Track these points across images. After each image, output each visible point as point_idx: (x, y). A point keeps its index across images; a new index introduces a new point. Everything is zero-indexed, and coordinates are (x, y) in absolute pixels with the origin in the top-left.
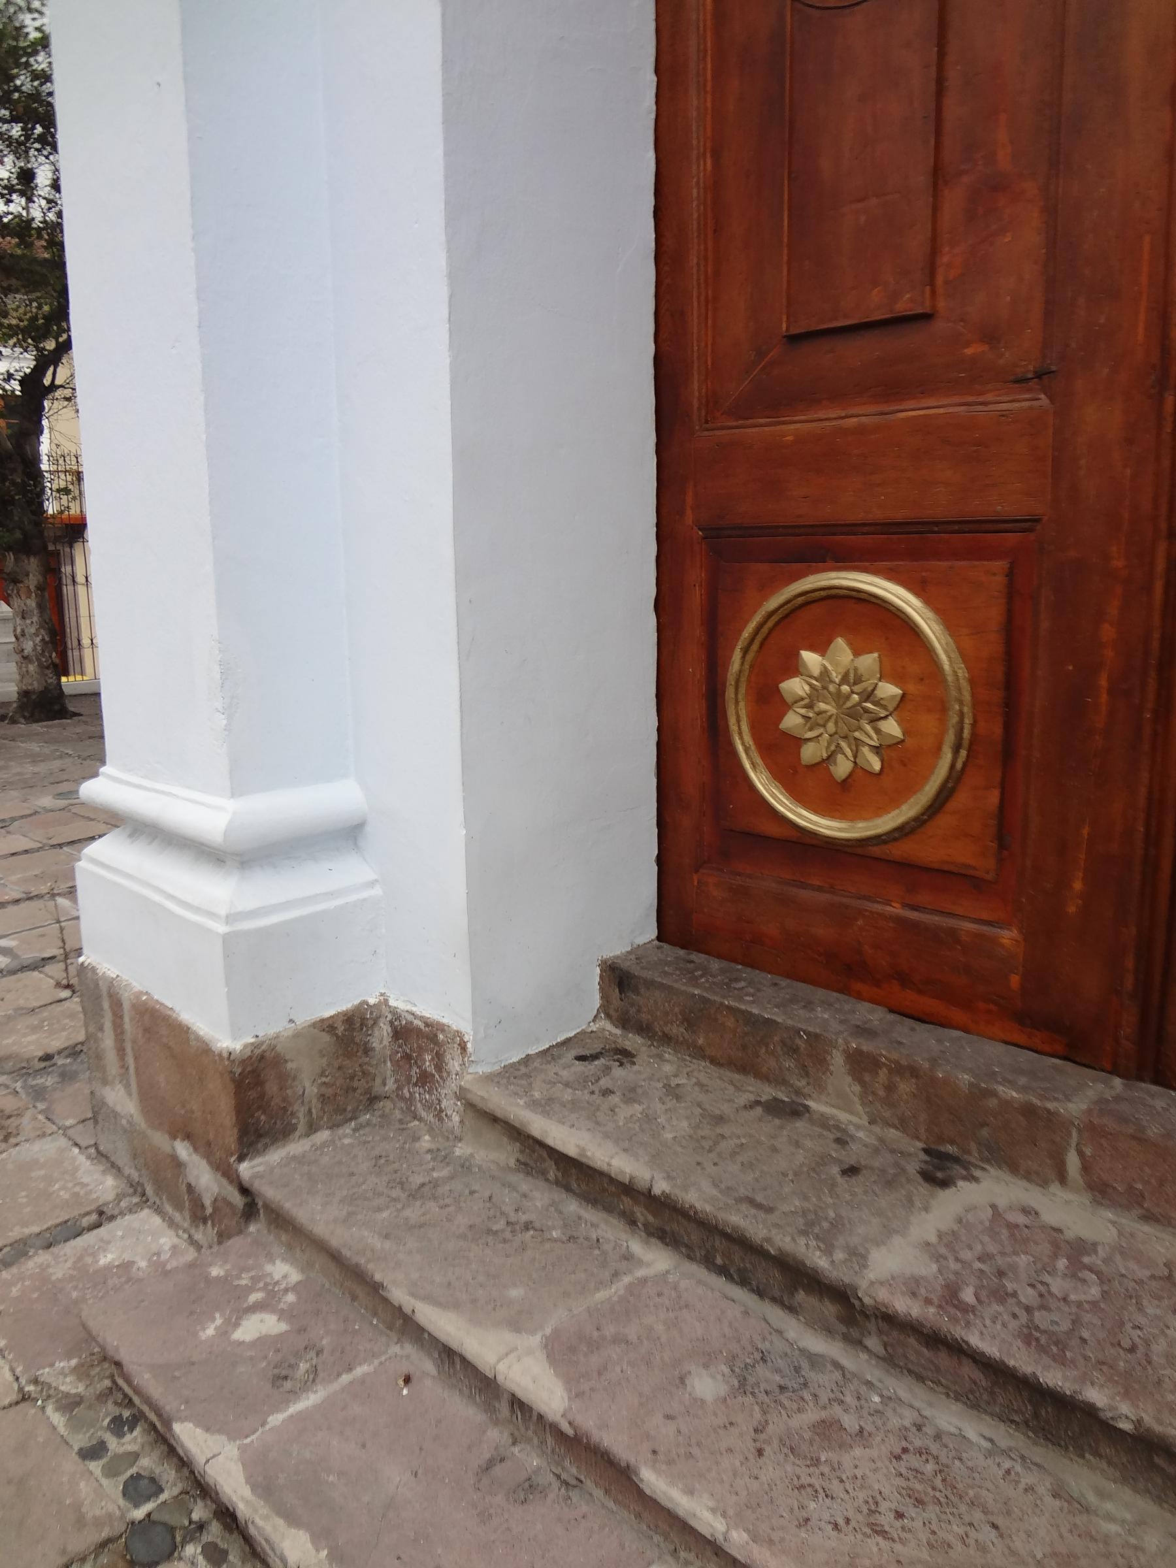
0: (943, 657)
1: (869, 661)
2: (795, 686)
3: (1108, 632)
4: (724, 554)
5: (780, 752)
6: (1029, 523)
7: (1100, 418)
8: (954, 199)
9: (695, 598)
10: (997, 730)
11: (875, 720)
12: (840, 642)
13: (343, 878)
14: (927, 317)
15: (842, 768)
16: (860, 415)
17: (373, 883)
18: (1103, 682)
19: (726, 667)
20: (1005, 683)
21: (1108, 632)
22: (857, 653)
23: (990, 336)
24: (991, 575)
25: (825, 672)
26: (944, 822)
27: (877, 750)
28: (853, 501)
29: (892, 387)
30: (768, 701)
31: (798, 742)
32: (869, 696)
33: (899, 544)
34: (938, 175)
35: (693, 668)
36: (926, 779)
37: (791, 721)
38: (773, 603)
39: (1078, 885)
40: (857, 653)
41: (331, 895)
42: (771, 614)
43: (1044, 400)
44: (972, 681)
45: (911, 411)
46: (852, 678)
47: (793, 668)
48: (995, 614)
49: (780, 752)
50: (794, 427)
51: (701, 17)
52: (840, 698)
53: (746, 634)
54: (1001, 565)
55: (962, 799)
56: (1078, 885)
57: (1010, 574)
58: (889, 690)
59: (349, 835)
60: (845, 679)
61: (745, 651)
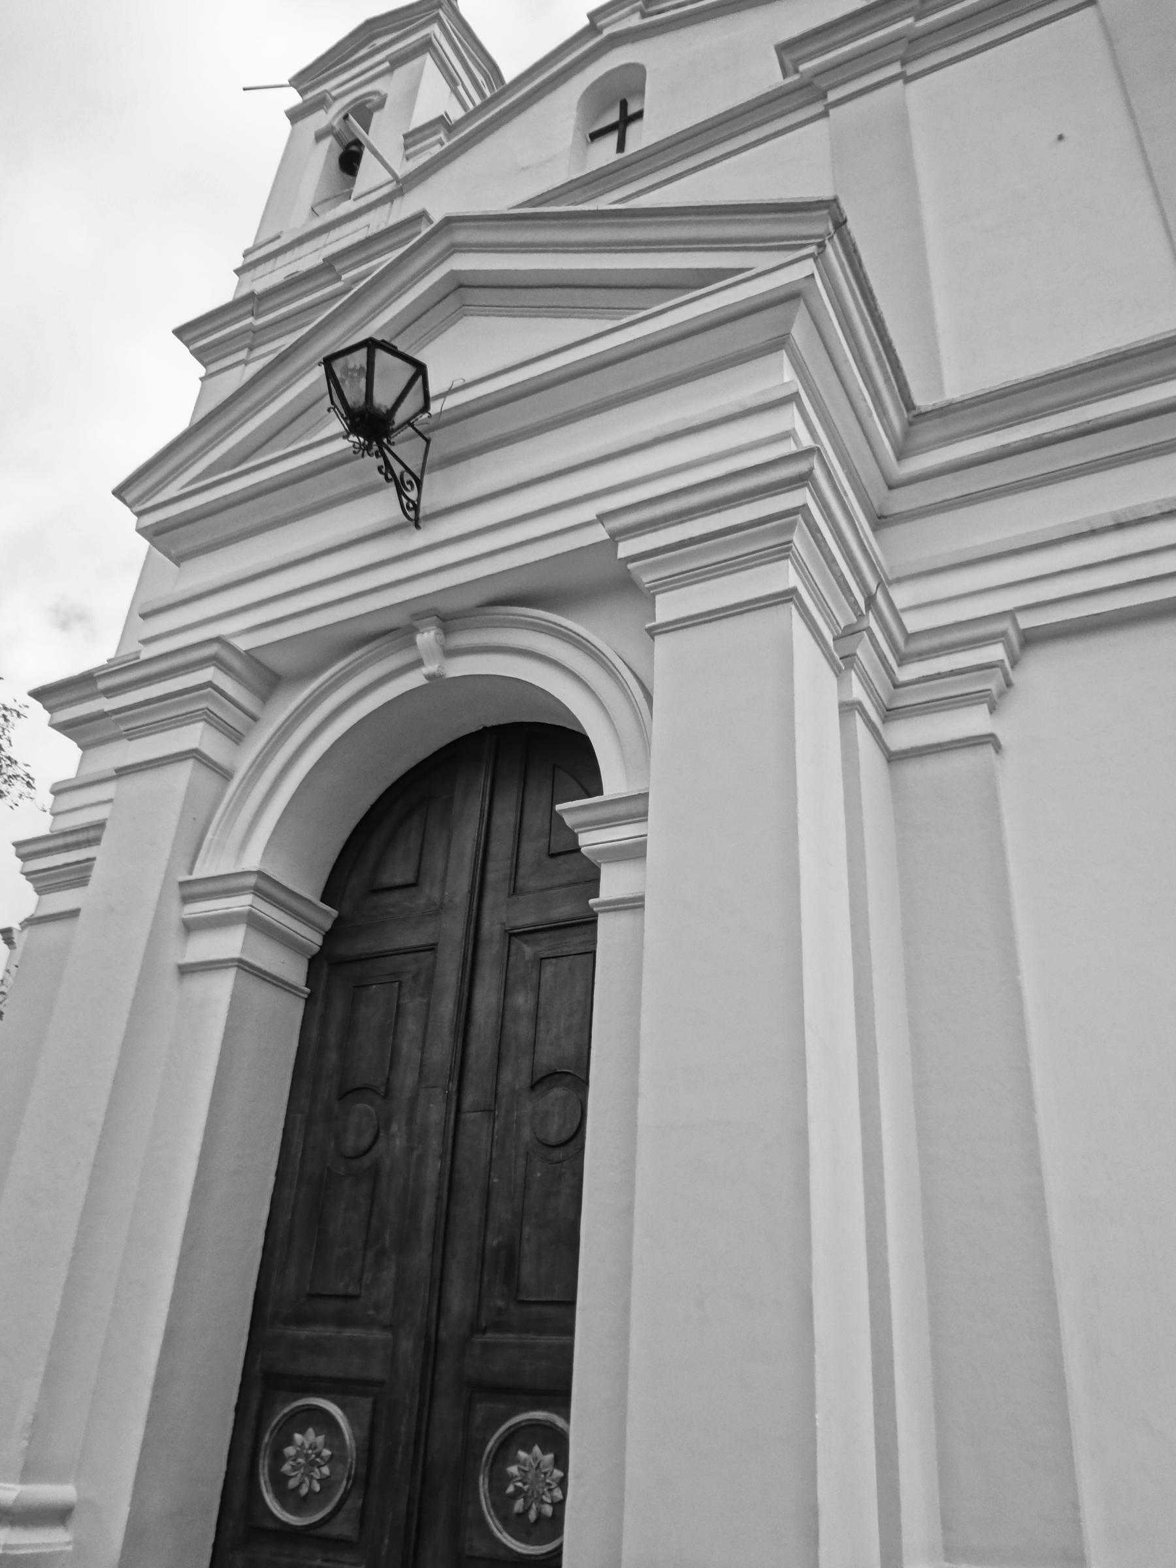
0: (347, 1437)
1: (321, 1439)
2: (290, 1451)
3: (403, 1429)
4: (270, 1384)
5: (279, 1481)
6: (381, 1383)
7: (407, 1345)
8: (370, 1255)
9: (254, 1406)
10: (363, 1470)
11: (320, 1467)
12: (311, 1431)
13: (53, 1539)
14: (356, 1297)
15: (304, 1490)
16: (329, 1331)
17: (68, 1543)
18: (400, 1449)
19: (262, 1438)
20: (368, 1448)
21: (403, 1429)
22: (317, 1435)
23: (377, 1307)
24: (366, 1403)
25: (303, 1444)
26: (341, 1516)
27: (319, 1481)
28: (325, 1367)
29: (343, 1321)
30: (278, 1458)
31: (287, 1478)
32: (318, 1455)
33: (337, 1388)
34: (367, 1245)
35: (247, 1442)
36: (335, 1495)
37: (286, 1468)
38: (286, 1410)
39: (386, 1541)
40: (317, 1435)
41: (49, 1545)
42: (285, 1415)
43: (390, 1336)
44: (357, 1449)
45: (348, 1333)
46: (313, 1447)
47: (290, 1442)
48: (366, 1420)
49: (279, 1481)
50: (306, 1333)
51: (333, 1037)
52: (307, 1456)
53: (274, 1423)
54: (371, 1400)
55: (349, 1504)
56: (386, 1541)
57: (375, 1404)
58: (327, 1453)
59: (59, 1515)
60: (310, 1448)
61: (272, 1432)
